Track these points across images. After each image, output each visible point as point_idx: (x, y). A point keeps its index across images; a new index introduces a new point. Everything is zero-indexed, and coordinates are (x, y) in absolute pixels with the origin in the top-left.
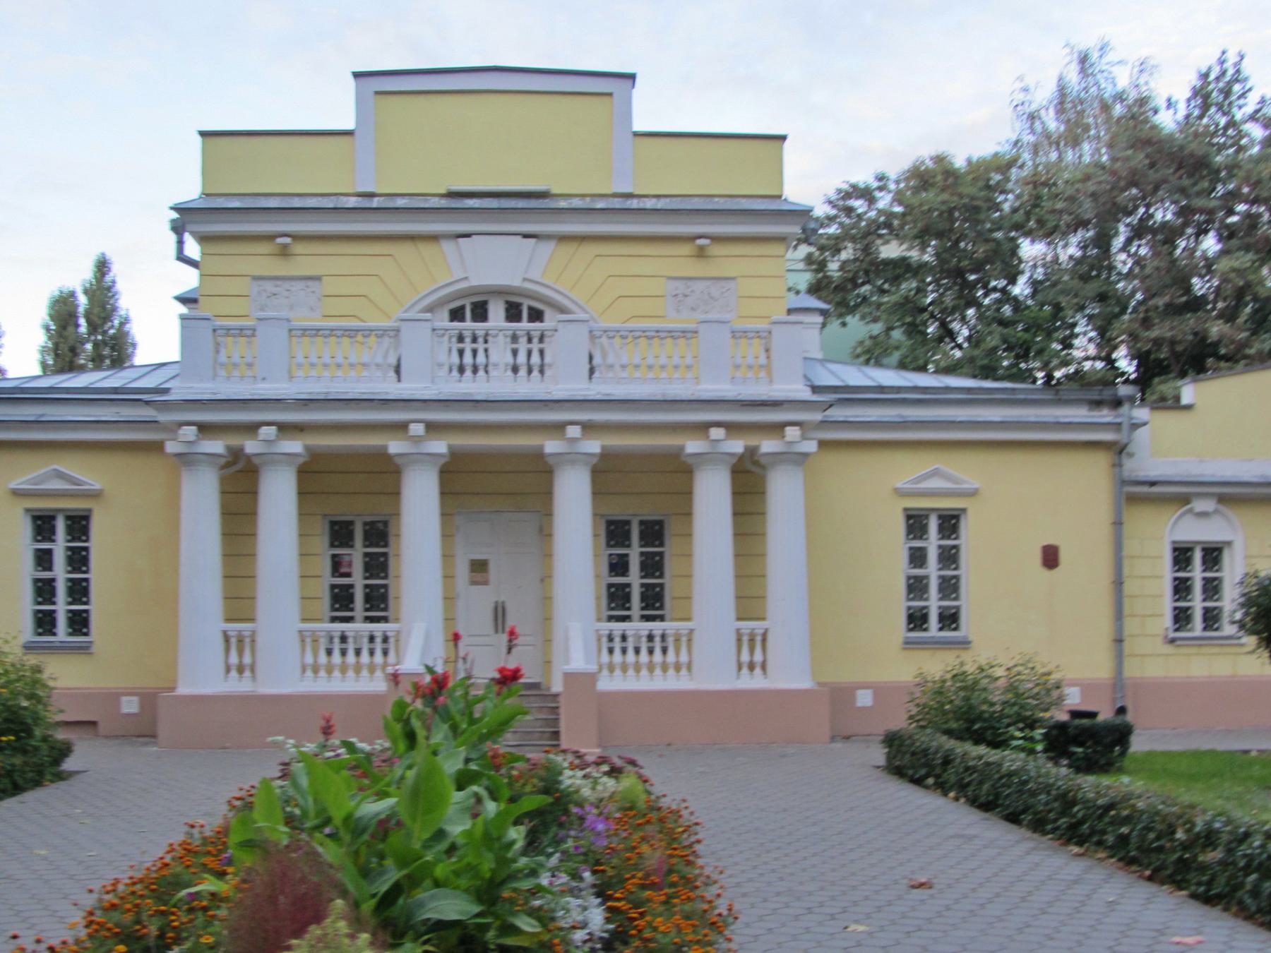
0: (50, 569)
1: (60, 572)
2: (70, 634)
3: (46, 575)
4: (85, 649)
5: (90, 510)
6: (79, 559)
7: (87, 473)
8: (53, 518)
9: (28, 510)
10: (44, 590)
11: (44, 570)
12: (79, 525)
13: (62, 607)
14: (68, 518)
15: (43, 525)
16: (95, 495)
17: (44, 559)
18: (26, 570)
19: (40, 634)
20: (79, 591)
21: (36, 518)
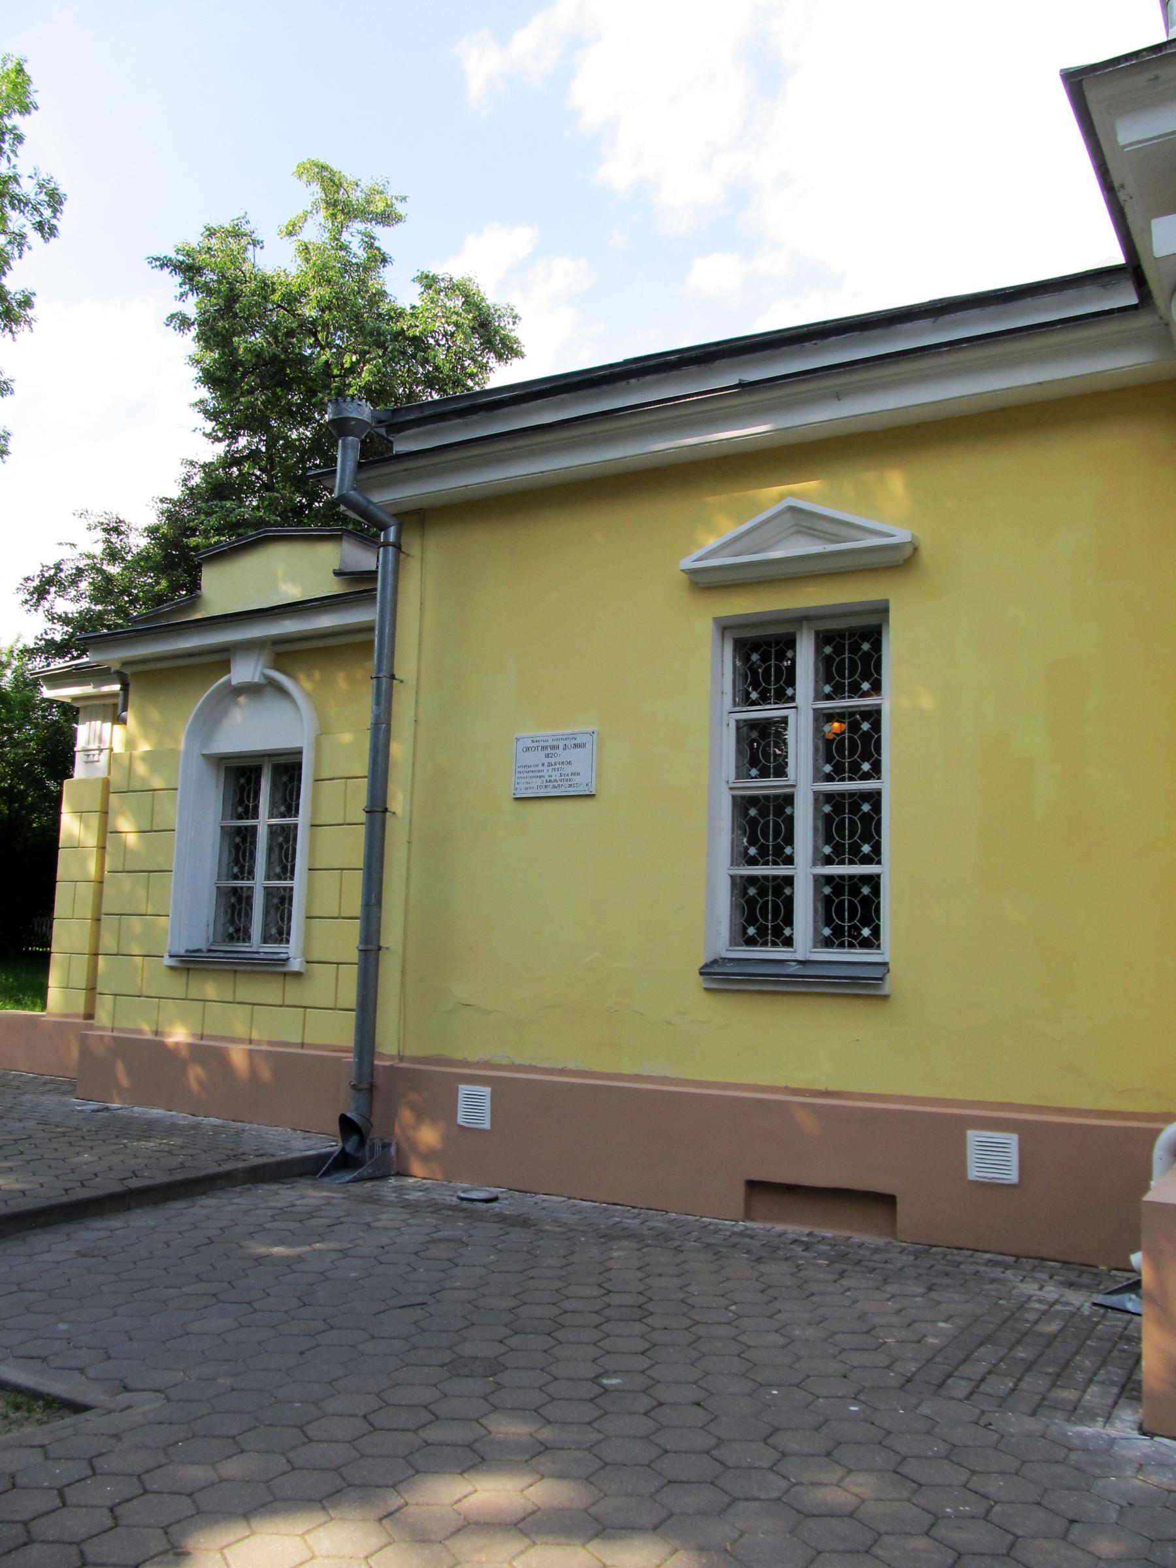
0: (781, 771)
1: (802, 777)
2: (828, 943)
3: (769, 786)
4: (866, 986)
5: (887, 602)
6: (855, 746)
7: (883, 504)
8: (790, 643)
9: (725, 627)
10: (762, 825)
11: (764, 774)
12: (854, 653)
13: (805, 869)
14: (823, 639)
15: (761, 661)
16: (898, 561)
17: (760, 747)
18: (707, 772)
19: (750, 942)
20: (854, 825)
21: (744, 648)
